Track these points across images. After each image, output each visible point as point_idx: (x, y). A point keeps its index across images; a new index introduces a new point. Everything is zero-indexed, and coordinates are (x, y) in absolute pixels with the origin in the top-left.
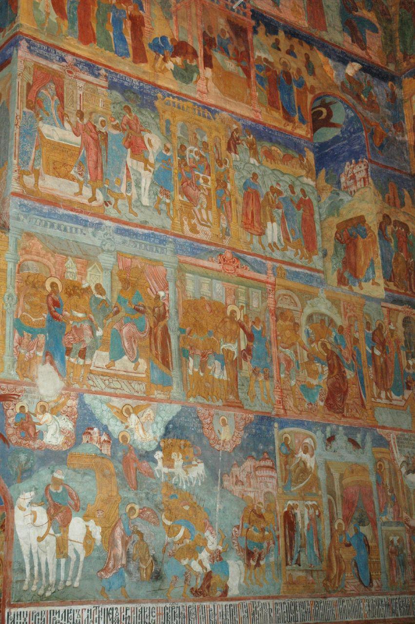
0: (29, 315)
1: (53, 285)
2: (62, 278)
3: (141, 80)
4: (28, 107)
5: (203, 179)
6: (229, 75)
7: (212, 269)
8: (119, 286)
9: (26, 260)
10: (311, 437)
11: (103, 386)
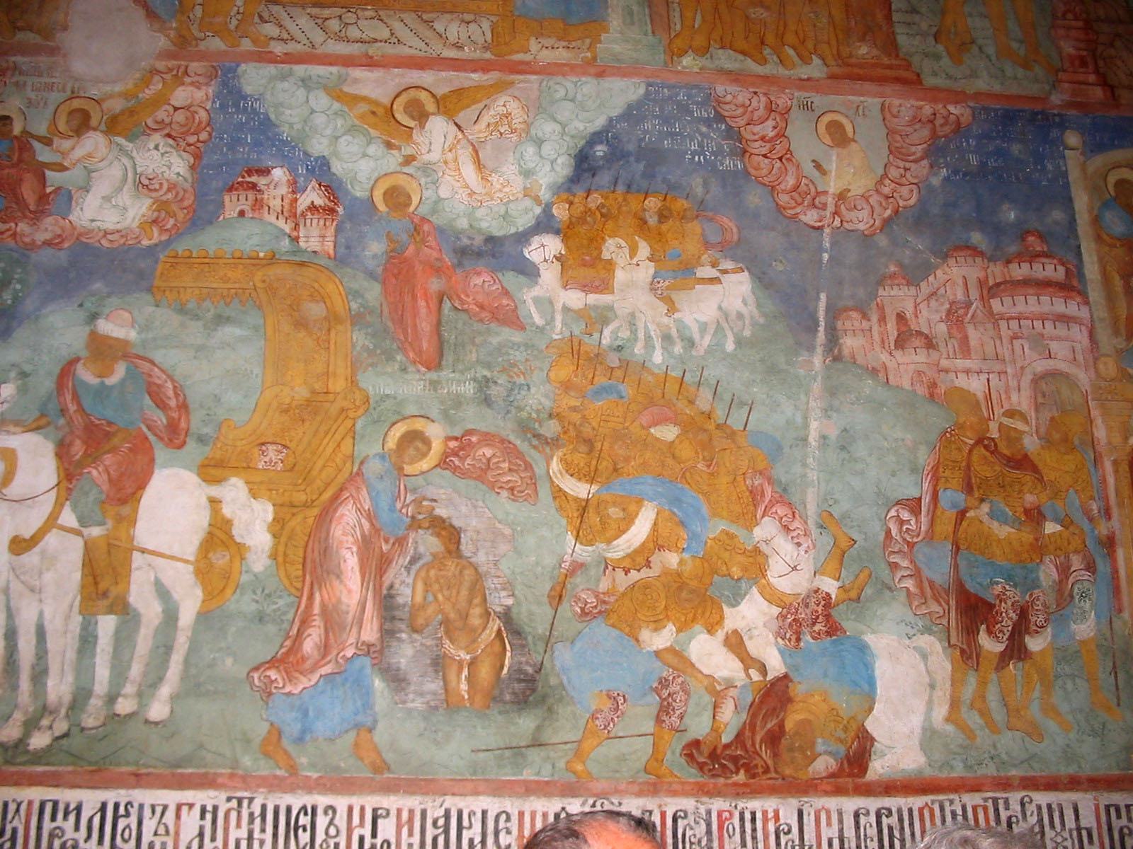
11: (318, 35)
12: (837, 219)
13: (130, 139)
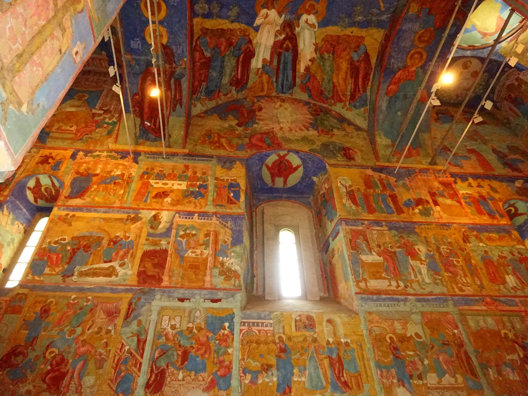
1: (391, 338)
2: (394, 333)
3: (404, 222)
4: (352, 250)
5: (456, 261)
6: (450, 206)
7: (481, 310)
8: (428, 332)
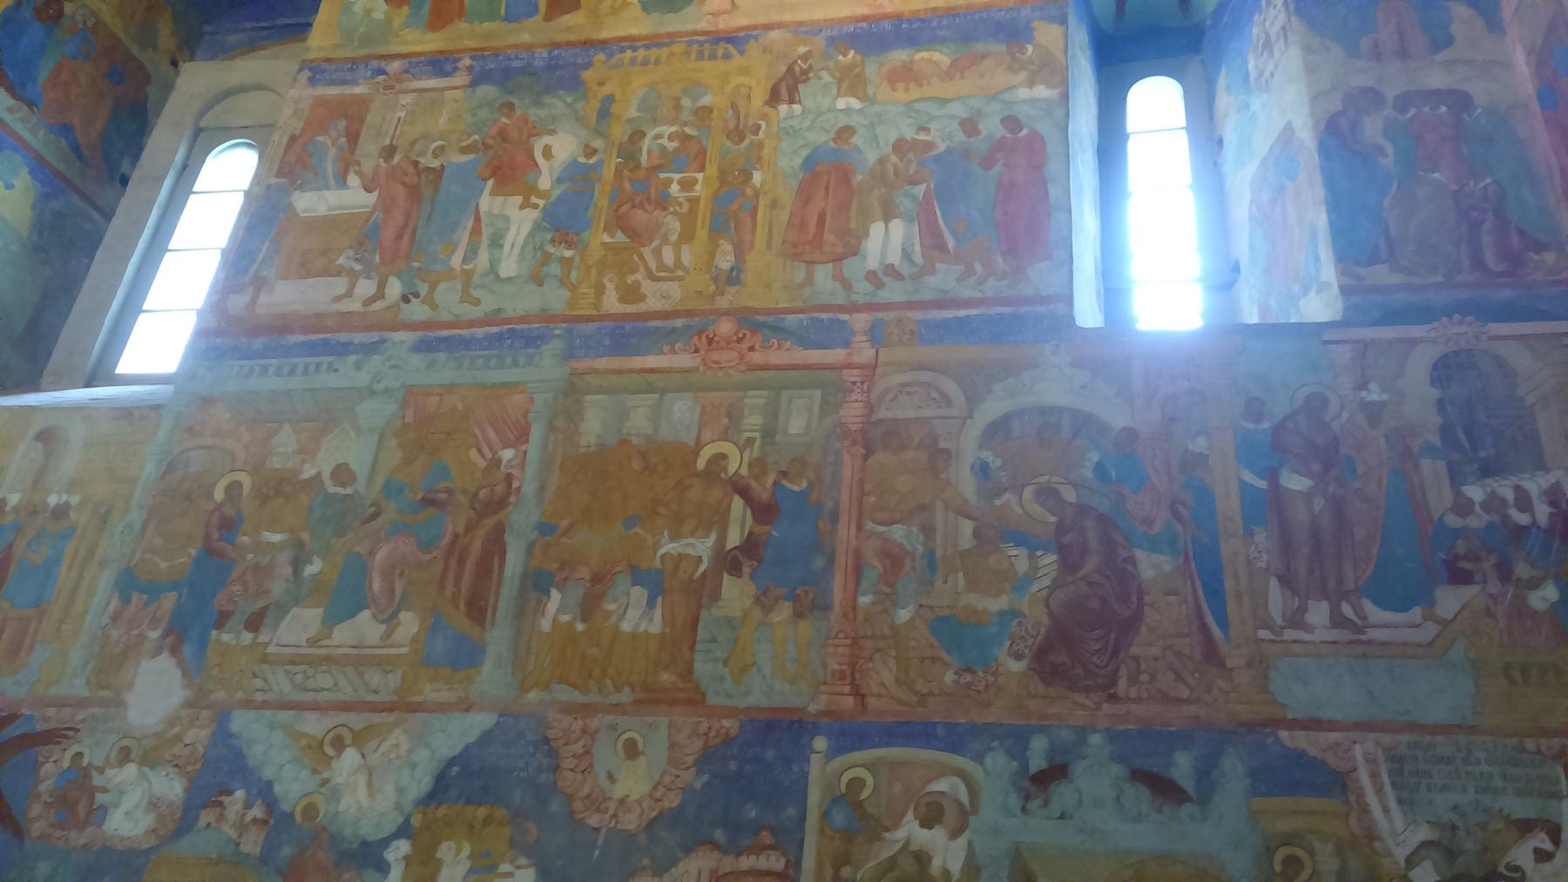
0: (157, 559)
9: (187, 450)
10: (962, 774)
11: (286, 687)
12: (614, 821)
13: (152, 768)
